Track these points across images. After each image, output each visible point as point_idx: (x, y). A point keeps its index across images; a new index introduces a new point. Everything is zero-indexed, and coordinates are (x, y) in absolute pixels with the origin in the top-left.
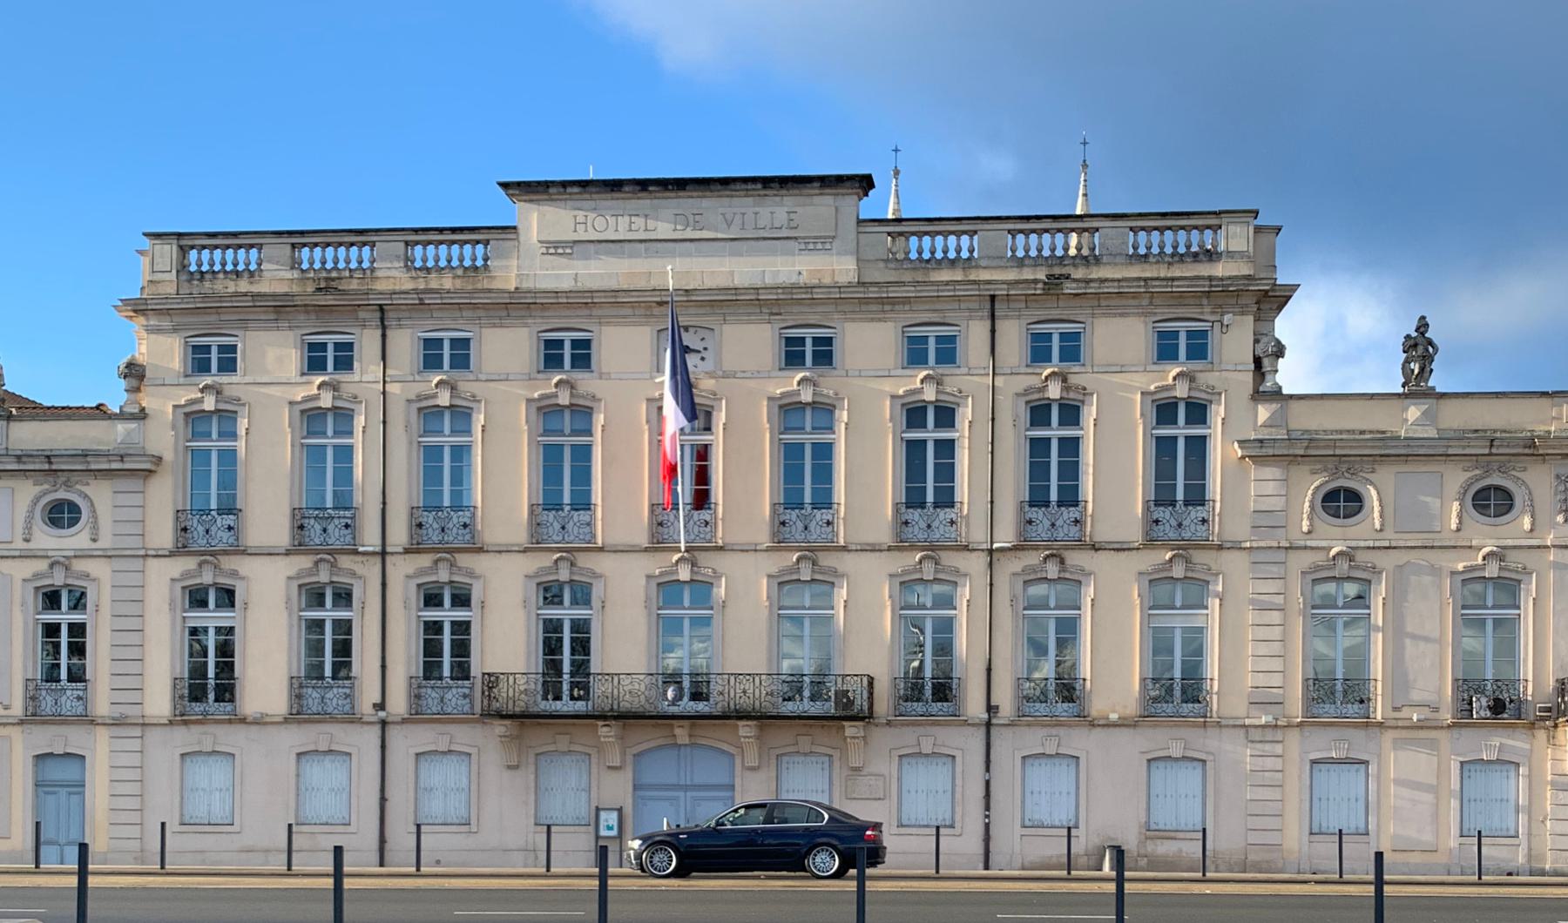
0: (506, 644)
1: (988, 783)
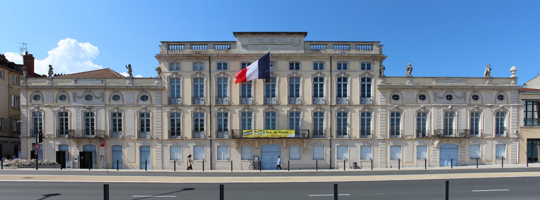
0: (235, 123)
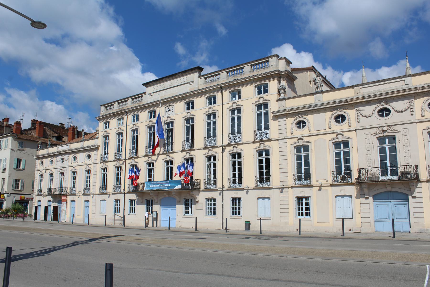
1: (222, 205)
